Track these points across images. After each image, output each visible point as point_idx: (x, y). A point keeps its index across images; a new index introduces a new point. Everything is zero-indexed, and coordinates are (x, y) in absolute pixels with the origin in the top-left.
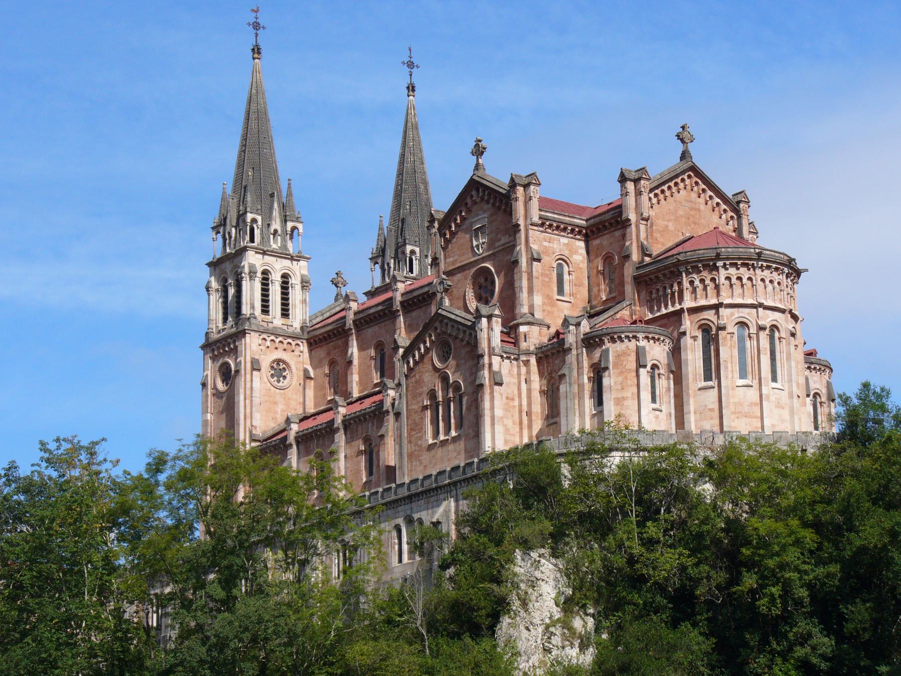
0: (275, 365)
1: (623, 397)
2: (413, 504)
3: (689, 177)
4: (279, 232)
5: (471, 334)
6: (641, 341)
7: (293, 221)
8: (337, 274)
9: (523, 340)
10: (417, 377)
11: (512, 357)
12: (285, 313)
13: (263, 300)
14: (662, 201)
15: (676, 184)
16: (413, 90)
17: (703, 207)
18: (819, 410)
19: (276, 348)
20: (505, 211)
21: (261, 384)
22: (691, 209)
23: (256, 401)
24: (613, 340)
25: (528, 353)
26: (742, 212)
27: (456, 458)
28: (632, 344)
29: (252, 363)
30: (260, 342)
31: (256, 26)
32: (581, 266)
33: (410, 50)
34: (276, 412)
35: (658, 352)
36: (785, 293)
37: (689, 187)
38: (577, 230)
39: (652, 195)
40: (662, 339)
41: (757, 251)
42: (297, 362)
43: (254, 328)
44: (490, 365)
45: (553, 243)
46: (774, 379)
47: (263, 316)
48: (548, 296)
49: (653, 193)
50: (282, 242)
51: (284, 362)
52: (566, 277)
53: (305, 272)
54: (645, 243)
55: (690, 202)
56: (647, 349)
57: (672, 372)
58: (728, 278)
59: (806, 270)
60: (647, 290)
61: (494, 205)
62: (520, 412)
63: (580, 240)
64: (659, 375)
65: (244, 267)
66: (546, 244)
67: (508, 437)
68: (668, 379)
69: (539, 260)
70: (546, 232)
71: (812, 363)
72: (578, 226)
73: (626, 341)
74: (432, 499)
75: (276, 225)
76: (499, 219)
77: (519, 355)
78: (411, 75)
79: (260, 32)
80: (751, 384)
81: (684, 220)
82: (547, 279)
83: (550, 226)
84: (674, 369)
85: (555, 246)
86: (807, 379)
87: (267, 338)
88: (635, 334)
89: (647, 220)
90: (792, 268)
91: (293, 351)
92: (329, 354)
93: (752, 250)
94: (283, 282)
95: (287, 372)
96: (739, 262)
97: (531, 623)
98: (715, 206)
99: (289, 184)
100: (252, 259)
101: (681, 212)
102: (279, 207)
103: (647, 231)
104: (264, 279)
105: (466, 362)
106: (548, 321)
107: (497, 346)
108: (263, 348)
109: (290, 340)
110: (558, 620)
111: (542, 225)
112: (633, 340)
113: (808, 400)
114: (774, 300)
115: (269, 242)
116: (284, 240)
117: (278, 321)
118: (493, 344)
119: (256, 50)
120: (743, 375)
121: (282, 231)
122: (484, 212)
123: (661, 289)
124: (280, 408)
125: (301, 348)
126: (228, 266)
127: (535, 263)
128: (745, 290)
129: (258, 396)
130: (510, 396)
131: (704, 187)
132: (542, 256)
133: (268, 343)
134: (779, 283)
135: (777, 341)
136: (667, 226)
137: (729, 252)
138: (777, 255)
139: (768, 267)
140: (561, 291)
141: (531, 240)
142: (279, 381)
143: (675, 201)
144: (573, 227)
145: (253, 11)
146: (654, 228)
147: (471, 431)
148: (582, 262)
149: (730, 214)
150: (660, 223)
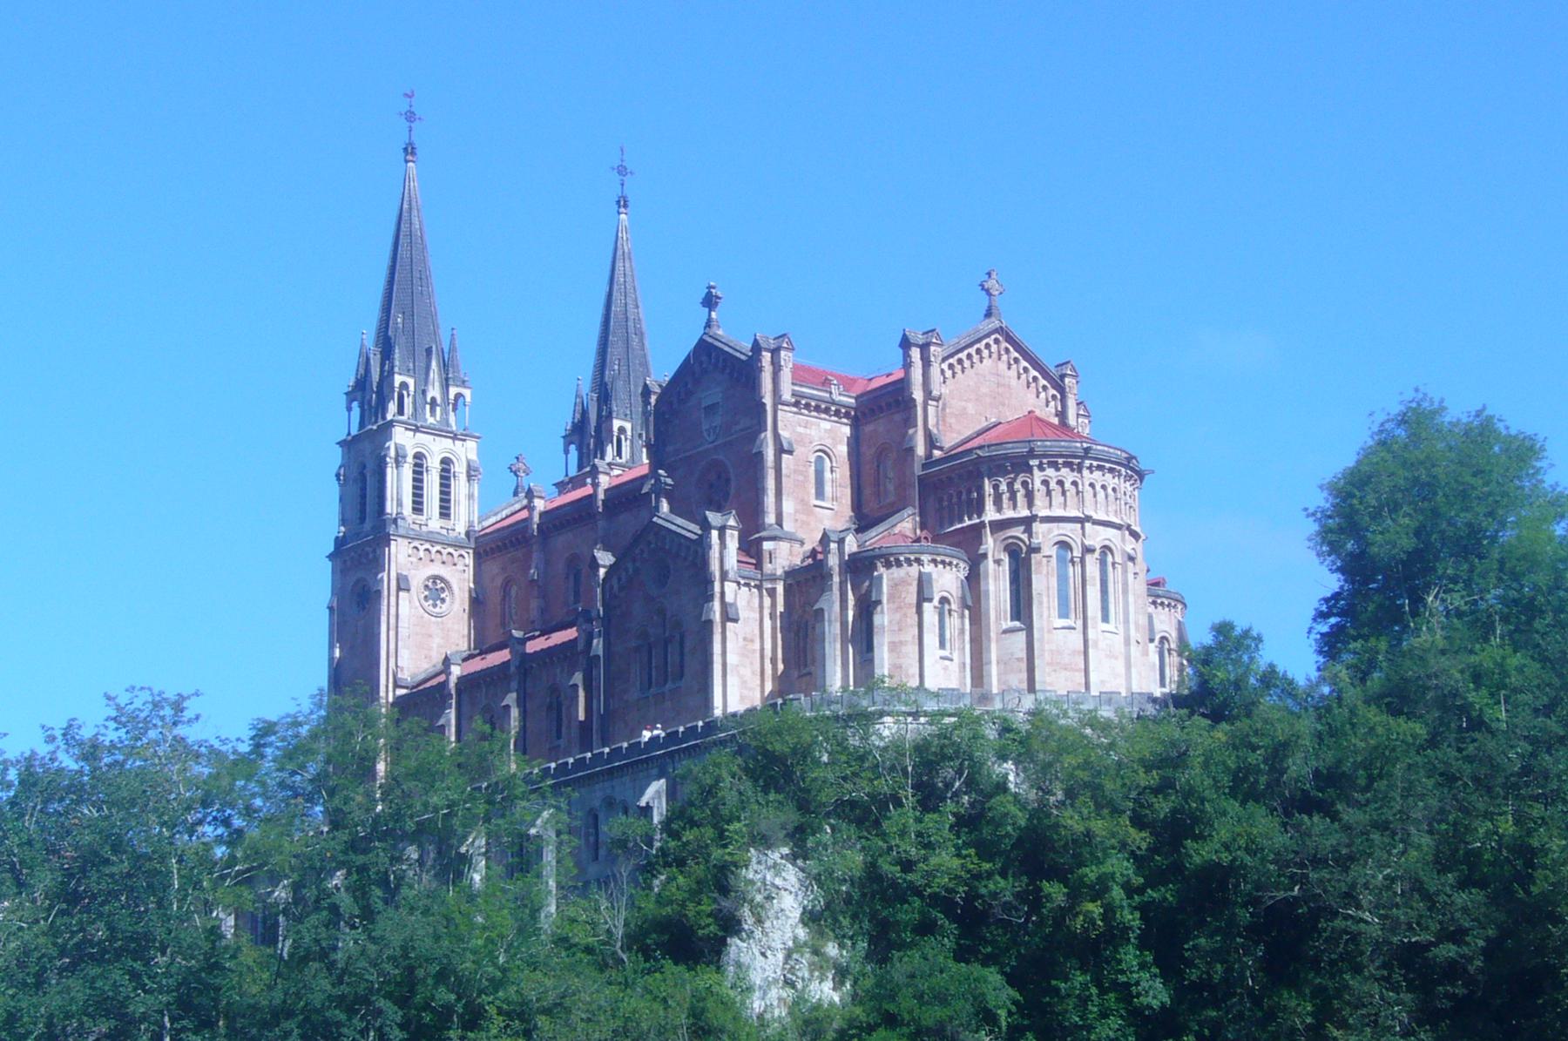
0: (430, 584)
1: (901, 642)
3: (997, 341)
4: (439, 401)
6: (926, 566)
7: (457, 386)
8: (517, 458)
9: (768, 560)
12: (445, 512)
13: (414, 495)
15: (979, 351)
17: (1014, 382)
18: (1167, 660)
19: (432, 561)
21: (411, 608)
23: (403, 632)
24: (888, 565)
25: (773, 579)
26: (1068, 390)
28: (914, 569)
29: (398, 580)
30: (410, 552)
33: (622, 150)
34: (430, 649)
35: (948, 580)
36: (1123, 502)
37: (995, 356)
38: (843, 411)
39: (945, 366)
40: (955, 563)
41: (1085, 445)
43: (401, 531)
44: (723, 594)
46: (1105, 619)
47: (415, 516)
48: (802, 500)
49: (947, 363)
50: (442, 414)
51: (442, 580)
52: (828, 475)
53: (473, 456)
54: (935, 431)
56: (934, 576)
57: (968, 607)
58: (1045, 483)
63: (846, 424)
64: (950, 611)
65: (389, 448)
66: (800, 430)
67: (746, 692)
68: (962, 616)
69: (790, 452)
70: (802, 414)
71: (1158, 596)
72: (844, 406)
75: (434, 392)
77: (761, 581)
78: (622, 185)
80: (1073, 625)
81: (988, 400)
82: (801, 478)
83: (807, 406)
84: (970, 603)
85: (813, 433)
86: (1150, 617)
87: (419, 546)
88: (917, 556)
89: (937, 399)
90: (1132, 469)
91: (455, 565)
92: (504, 569)
93: (1078, 445)
94: (443, 470)
95: (447, 593)
97: (769, 948)
98: (1031, 380)
99: (453, 335)
100: (401, 437)
101: (984, 390)
102: (439, 366)
103: (937, 416)
104: (416, 465)
106: (800, 535)
107: (733, 568)
109: (451, 550)
110: (805, 944)
112: (915, 565)
113: (1152, 647)
115: (425, 414)
116: (445, 412)
117: (435, 524)
118: (727, 566)
119: (410, 150)
120: (1064, 614)
121: (443, 399)
123: (955, 494)
124: (436, 641)
126: (367, 447)
127: (785, 456)
129: (406, 625)
130: (749, 636)
131: (1017, 355)
132: (795, 446)
133: (421, 554)
135: (1110, 568)
136: (965, 409)
137: (1046, 446)
138: (1111, 450)
139: (1100, 468)
140: (820, 493)
141: (780, 424)
142: (435, 606)
143: (977, 374)
145: (406, 95)
146: (948, 410)
149: (1052, 392)
150: (955, 405)
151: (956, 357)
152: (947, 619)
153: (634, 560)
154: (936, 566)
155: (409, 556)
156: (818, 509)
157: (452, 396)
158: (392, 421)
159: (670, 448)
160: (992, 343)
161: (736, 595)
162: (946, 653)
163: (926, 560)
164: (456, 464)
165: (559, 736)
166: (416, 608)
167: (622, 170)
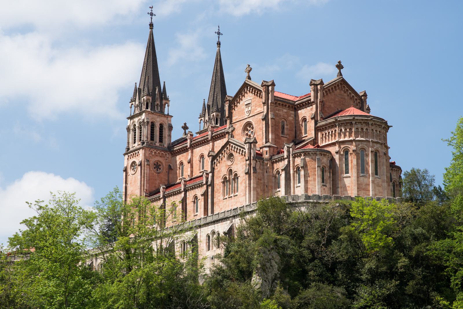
0: (156, 164)
2: (216, 225)
5: (243, 151)
6: (318, 155)
10: (219, 169)
11: (261, 161)
12: (161, 140)
14: (329, 94)
16: (220, 45)
17: (346, 98)
18: (396, 188)
20: (260, 97)
22: (341, 98)
27: (235, 205)
30: (150, 153)
31: (152, 14)
32: (292, 122)
37: (340, 89)
39: (324, 92)
40: (327, 154)
42: (166, 162)
45: (280, 111)
47: (151, 141)
48: (277, 135)
50: (160, 109)
51: (160, 162)
52: (286, 127)
55: (341, 95)
59: (392, 126)
60: (321, 133)
61: (254, 94)
62: (264, 185)
63: (292, 110)
66: (277, 112)
68: (330, 173)
70: (277, 107)
71: (393, 168)
73: (312, 155)
74: (224, 223)
75: (158, 102)
76: (257, 100)
78: (219, 38)
79: (153, 17)
82: (277, 127)
85: (281, 113)
86: (391, 174)
91: (164, 157)
95: (161, 166)
96: (362, 122)
97: (267, 278)
99: (164, 84)
101: (337, 100)
105: (240, 163)
108: (151, 155)
109: (163, 153)
111: (276, 103)
113: (391, 184)
114: (377, 139)
117: (158, 144)
122: (250, 97)
125: (168, 156)
126: (136, 120)
128: (364, 134)
130: (260, 178)
131: (347, 88)
133: (153, 153)
134: (379, 132)
135: (378, 158)
136: (330, 105)
140: (283, 132)
142: (157, 170)
143: (334, 94)
144: (289, 105)
145: (150, 7)
147: (242, 193)
148: (293, 120)
149: (358, 101)
151: (328, 89)
152: (325, 173)
153: (222, 154)
154: (321, 155)
155: (149, 154)
156: (282, 138)
157: (163, 103)
158: (145, 111)
159: (233, 118)
160: (339, 84)
161: (256, 165)
162: (324, 184)
163: (318, 154)
164: (165, 125)
165: (197, 212)
166: (151, 171)
167: (219, 33)
